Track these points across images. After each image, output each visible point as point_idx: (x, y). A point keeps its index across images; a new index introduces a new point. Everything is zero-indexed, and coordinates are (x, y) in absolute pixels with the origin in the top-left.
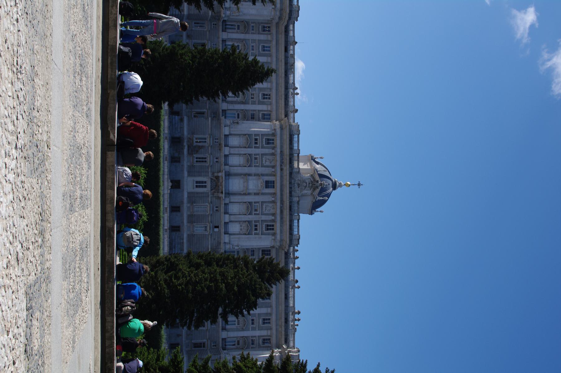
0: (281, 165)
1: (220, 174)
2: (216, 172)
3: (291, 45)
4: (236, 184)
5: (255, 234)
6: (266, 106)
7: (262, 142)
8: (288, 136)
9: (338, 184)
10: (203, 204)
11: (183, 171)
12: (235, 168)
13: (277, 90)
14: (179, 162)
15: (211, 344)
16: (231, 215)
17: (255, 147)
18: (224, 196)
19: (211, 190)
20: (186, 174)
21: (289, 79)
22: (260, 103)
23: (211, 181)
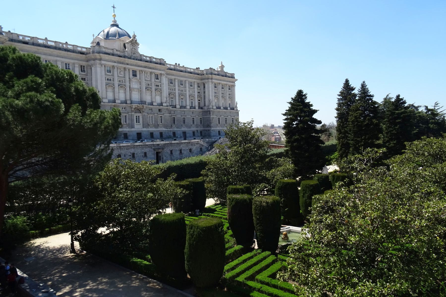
1: (134, 107)
3: (19, 38)
4: (136, 97)
5: (161, 87)
7: (109, 75)
8: (106, 55)
9: (115, 23)
11: (132, 131)
12: (127, 96)
13: (63, 58)
14: (126, 134)
15: (200, 115)
17: (113, 81)
19: (141, 113)
20: (133, 129)
21: (52, 45)
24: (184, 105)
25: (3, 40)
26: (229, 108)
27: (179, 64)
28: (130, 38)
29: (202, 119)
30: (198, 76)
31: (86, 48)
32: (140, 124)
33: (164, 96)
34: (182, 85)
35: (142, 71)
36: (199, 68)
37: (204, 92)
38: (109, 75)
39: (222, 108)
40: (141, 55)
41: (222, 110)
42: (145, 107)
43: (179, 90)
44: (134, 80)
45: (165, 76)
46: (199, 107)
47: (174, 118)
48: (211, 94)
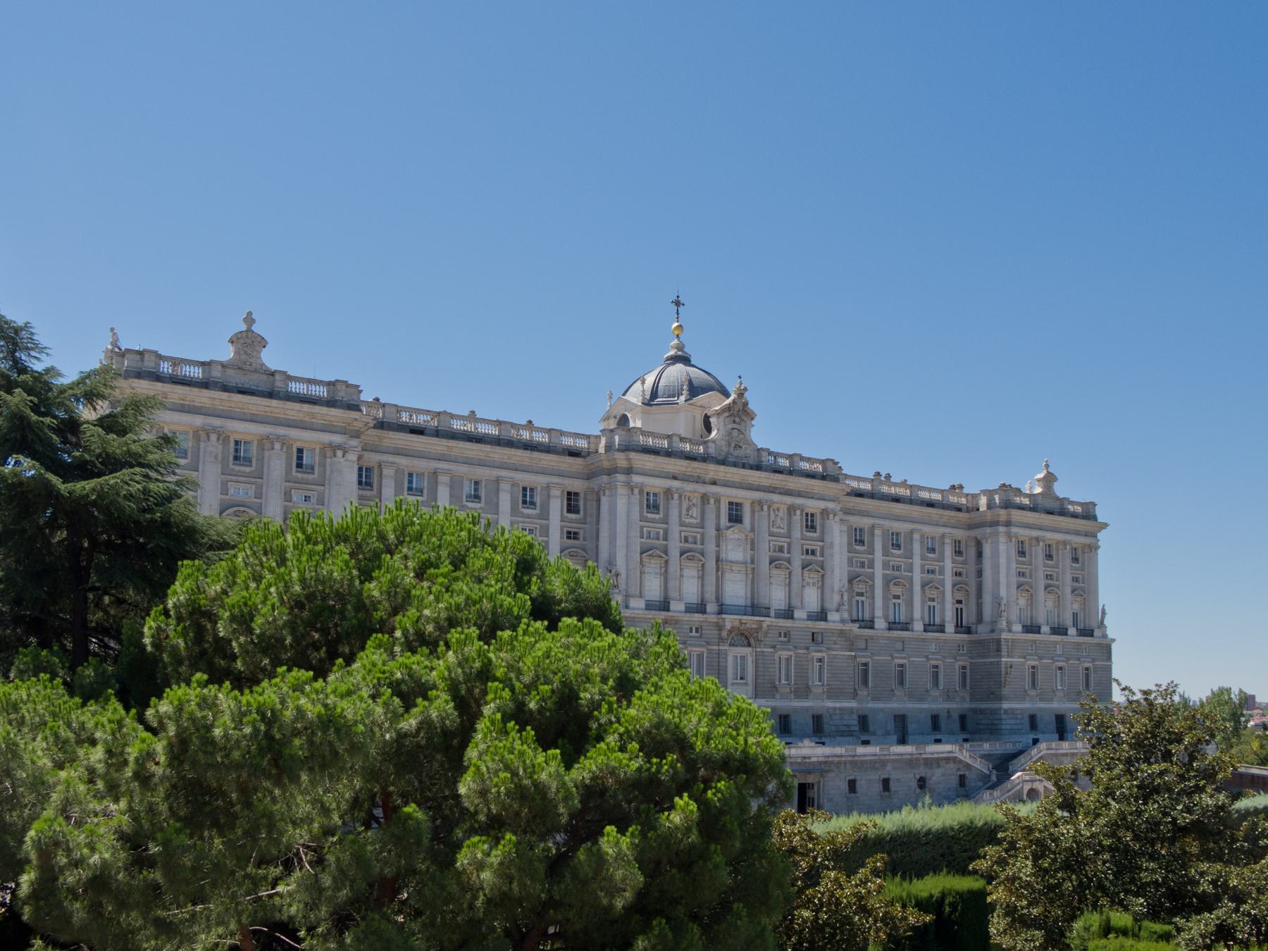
0: (704, 483)
1: (728, 626)
2: (720, 634)
4: (736, 590)
5: (822, 555)
6: (551, 500)
7: (653, 521)
9: (680, 353)
10: (777, 666)
13: (516, 470)
15: (962, 655)
16: (789, 604)
17: (666, 539)
18: (767, 619)
22: (545, 515)
23: (733, 645)
24: (903, 619)
25: (361, 425)
26: (1072, 631)
27: (888, 476)
28: (727, 395)
29: (968, 671)
30: (960, 514)
31: (588, 437)
32: (746, 684)
33: (833, 589)
34: (898, 546)
35: (760, 503)
36: (961, 487)
37: (980, 573)
38: (653, 521)
39: (1045, 629)
40: (758, 450)
41: (1045, 636)
42: (765, 626)
43: (885, 565)
44: (734, 534)
45: (837, 518)
46: (957, 626)
47: (866, 665)
48: (1003, 579)
